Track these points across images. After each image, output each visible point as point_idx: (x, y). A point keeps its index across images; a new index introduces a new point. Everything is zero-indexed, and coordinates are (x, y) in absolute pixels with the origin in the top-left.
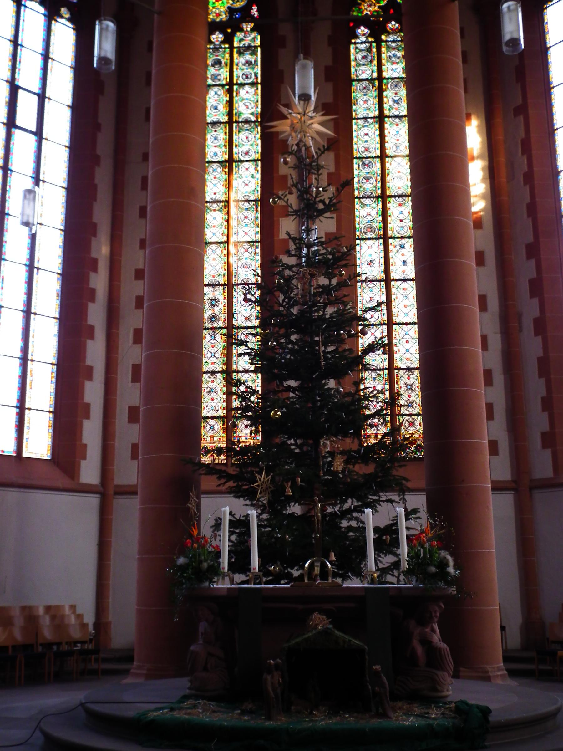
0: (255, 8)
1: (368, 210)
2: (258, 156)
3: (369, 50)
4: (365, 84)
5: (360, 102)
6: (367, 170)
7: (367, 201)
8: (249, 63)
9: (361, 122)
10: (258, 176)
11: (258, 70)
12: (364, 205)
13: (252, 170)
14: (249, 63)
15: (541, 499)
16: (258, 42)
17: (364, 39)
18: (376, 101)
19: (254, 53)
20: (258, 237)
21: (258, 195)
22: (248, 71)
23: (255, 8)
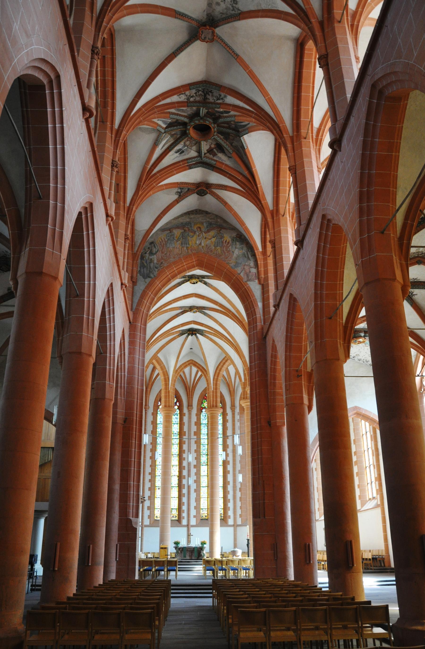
0: (178, 403)
1: (204, 458)
2: (178, 443)
3: (205, 416)
4: (204, 425)
5: (203, 430)
6: (204, 448)
7: (203, 456)
8: (176, 418)
9: (203, 435)
10: (178, 448)
11: (179, 420)
12: (203, 457)
13: (177, 447)
14: (176, 418)
15: (239, 528)
16: (179, 412)
17: (204, 413)
18: (207, 430)
19: (177, 415)
20: (178, 464)
21: (178, 453)
22: (176, 420)
23: (178, 403)
